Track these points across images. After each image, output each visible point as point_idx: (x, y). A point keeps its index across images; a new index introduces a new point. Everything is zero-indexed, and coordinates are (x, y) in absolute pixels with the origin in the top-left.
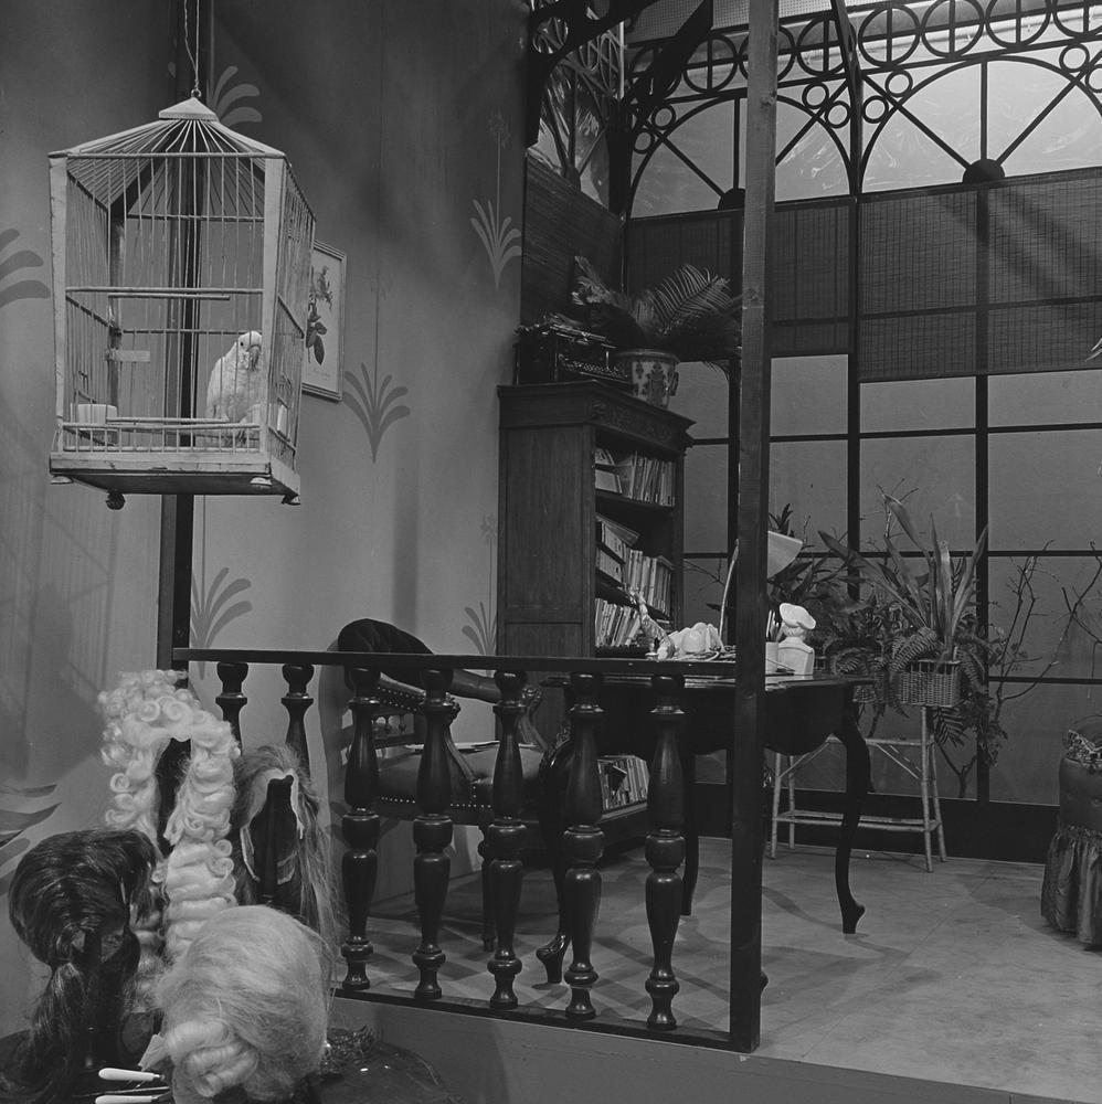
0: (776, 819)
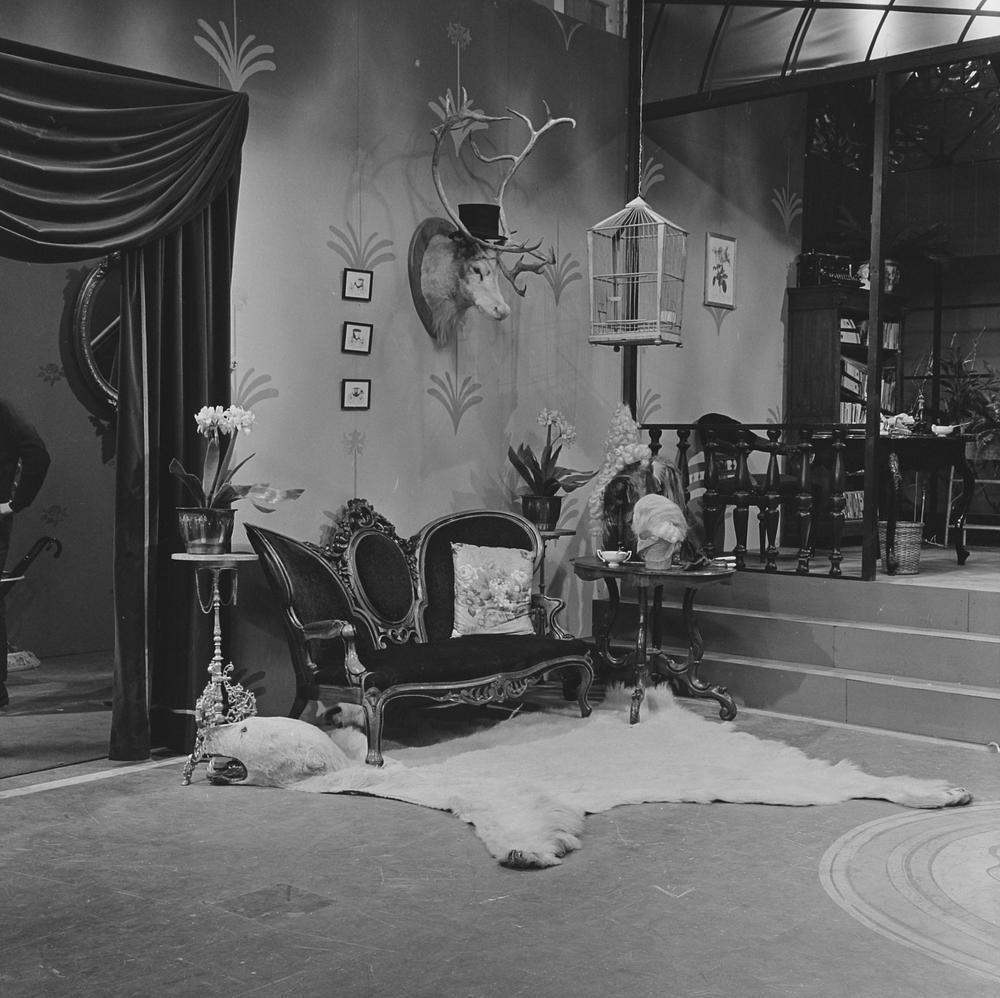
0: (948, 526)
